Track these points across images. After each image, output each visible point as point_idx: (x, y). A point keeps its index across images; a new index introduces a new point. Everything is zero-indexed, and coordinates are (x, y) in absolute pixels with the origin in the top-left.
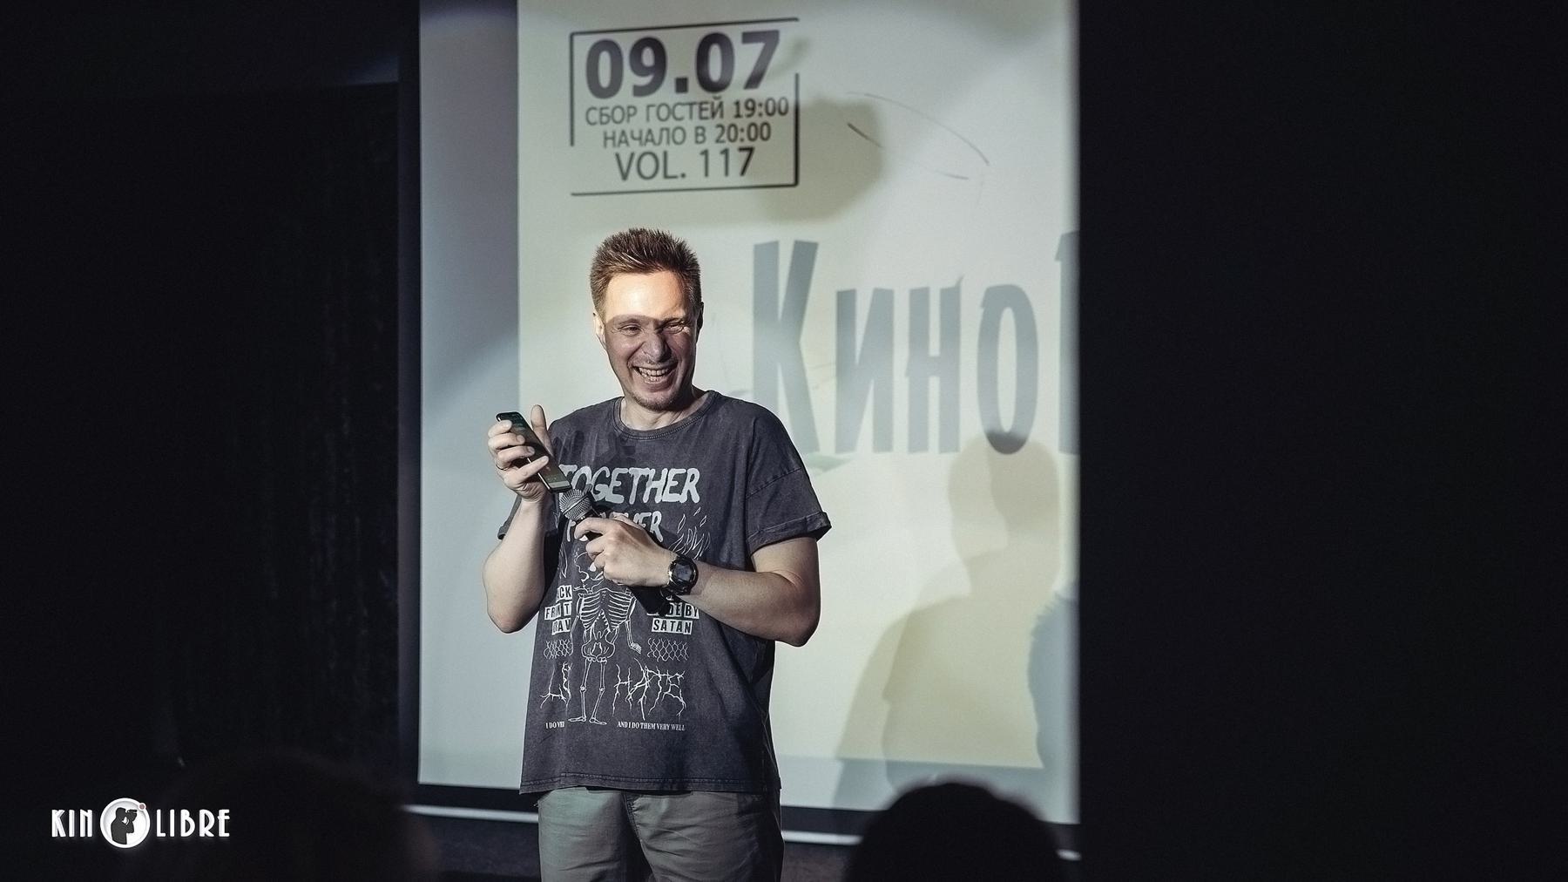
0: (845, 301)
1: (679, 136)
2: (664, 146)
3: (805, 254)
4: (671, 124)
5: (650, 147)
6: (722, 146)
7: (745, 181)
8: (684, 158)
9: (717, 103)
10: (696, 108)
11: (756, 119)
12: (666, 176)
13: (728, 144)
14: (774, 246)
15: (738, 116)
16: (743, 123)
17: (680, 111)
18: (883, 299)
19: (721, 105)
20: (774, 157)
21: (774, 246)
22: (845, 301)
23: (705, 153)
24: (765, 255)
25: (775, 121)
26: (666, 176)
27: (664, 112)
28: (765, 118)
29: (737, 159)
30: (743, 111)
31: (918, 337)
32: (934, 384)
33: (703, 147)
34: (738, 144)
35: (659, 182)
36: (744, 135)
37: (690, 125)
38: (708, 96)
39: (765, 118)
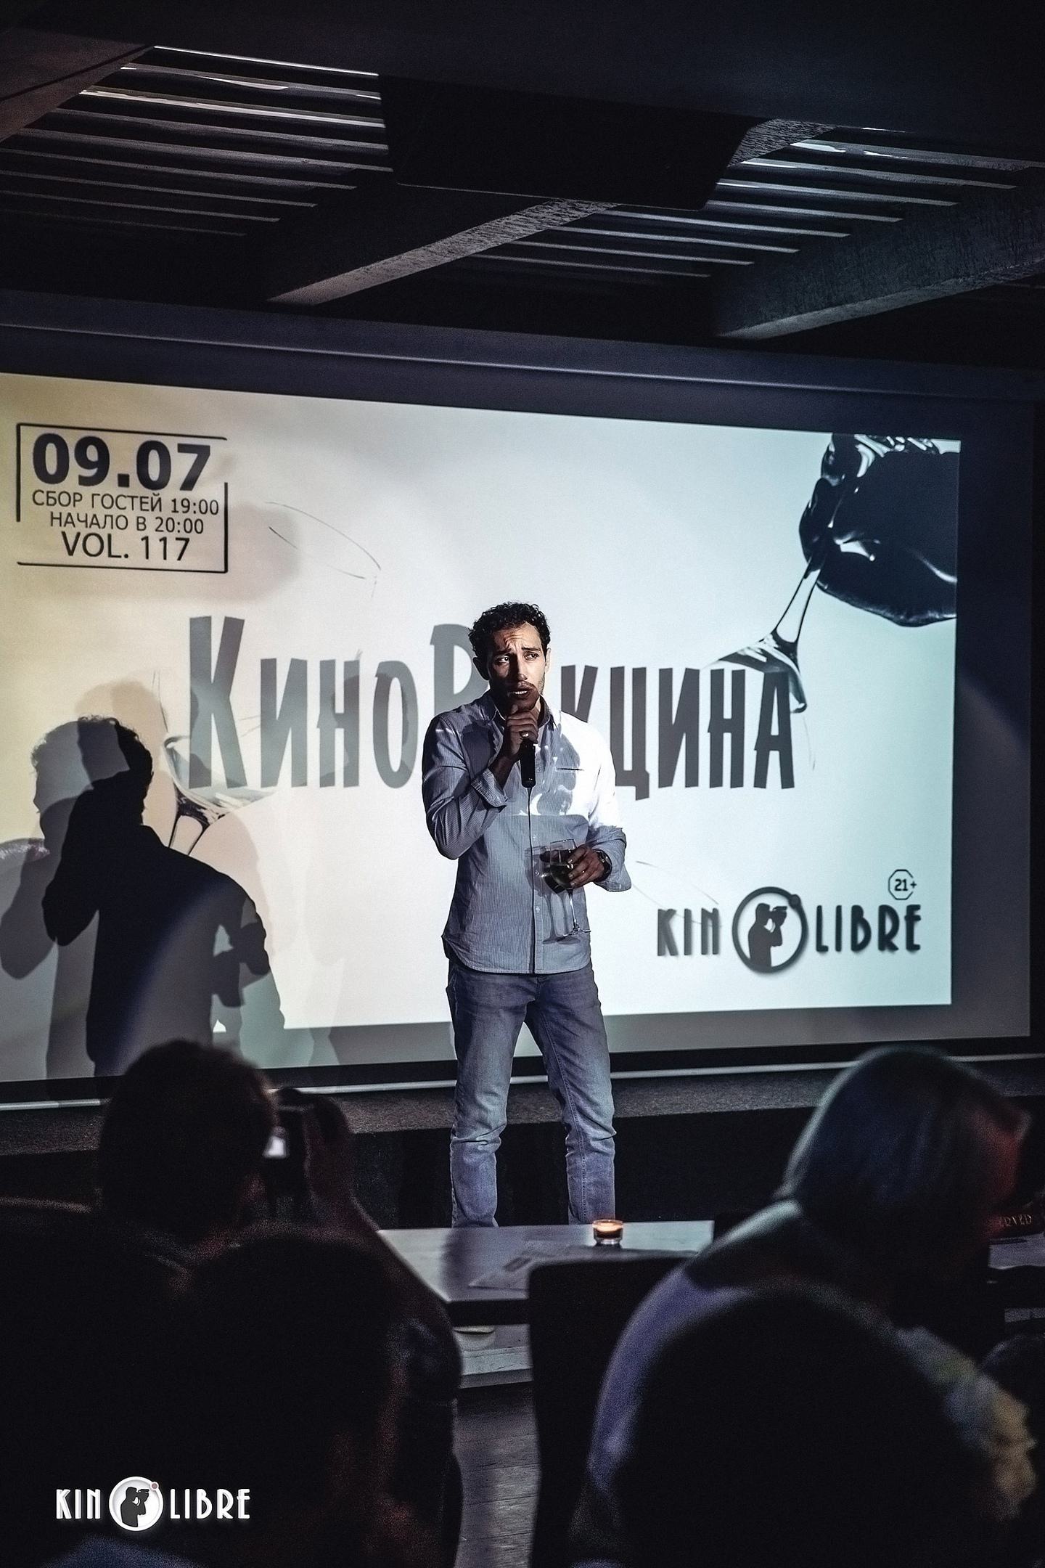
0: (268, 668)
1: (122, 522)
2: (108, 530)
3: (234, 629)
4: (115, 512)
5: (94, 529)
6: (162, 535)
7: (178, 565)
8: (127, 541)
9: (155, 499)
10: (137, 501)
11: (190, 515)
12: (110, 555)
13: (166, 534)
14: (207, 620)
15: (175, 511)
16: (180, 517)
17: (122, 502)
18: (298, 668)
19: (160, 500)
20: (205, 548)
21: (207, 620)
22: (268, 668)
23: (146, 539)
24: (200, 627)
25: (207, 518)
26: (110, 555)
27: (108, 502)
28: (199, 516)
29: (174, 547)
30: (179, 507)
31: (327, 697)
32: (339, 734)
33: (143, 534)
34: (175, 534)
35: (104, 559)
36: (181, 527)
37: (132, 515)
38: (149, 493)
39: (199, 516)
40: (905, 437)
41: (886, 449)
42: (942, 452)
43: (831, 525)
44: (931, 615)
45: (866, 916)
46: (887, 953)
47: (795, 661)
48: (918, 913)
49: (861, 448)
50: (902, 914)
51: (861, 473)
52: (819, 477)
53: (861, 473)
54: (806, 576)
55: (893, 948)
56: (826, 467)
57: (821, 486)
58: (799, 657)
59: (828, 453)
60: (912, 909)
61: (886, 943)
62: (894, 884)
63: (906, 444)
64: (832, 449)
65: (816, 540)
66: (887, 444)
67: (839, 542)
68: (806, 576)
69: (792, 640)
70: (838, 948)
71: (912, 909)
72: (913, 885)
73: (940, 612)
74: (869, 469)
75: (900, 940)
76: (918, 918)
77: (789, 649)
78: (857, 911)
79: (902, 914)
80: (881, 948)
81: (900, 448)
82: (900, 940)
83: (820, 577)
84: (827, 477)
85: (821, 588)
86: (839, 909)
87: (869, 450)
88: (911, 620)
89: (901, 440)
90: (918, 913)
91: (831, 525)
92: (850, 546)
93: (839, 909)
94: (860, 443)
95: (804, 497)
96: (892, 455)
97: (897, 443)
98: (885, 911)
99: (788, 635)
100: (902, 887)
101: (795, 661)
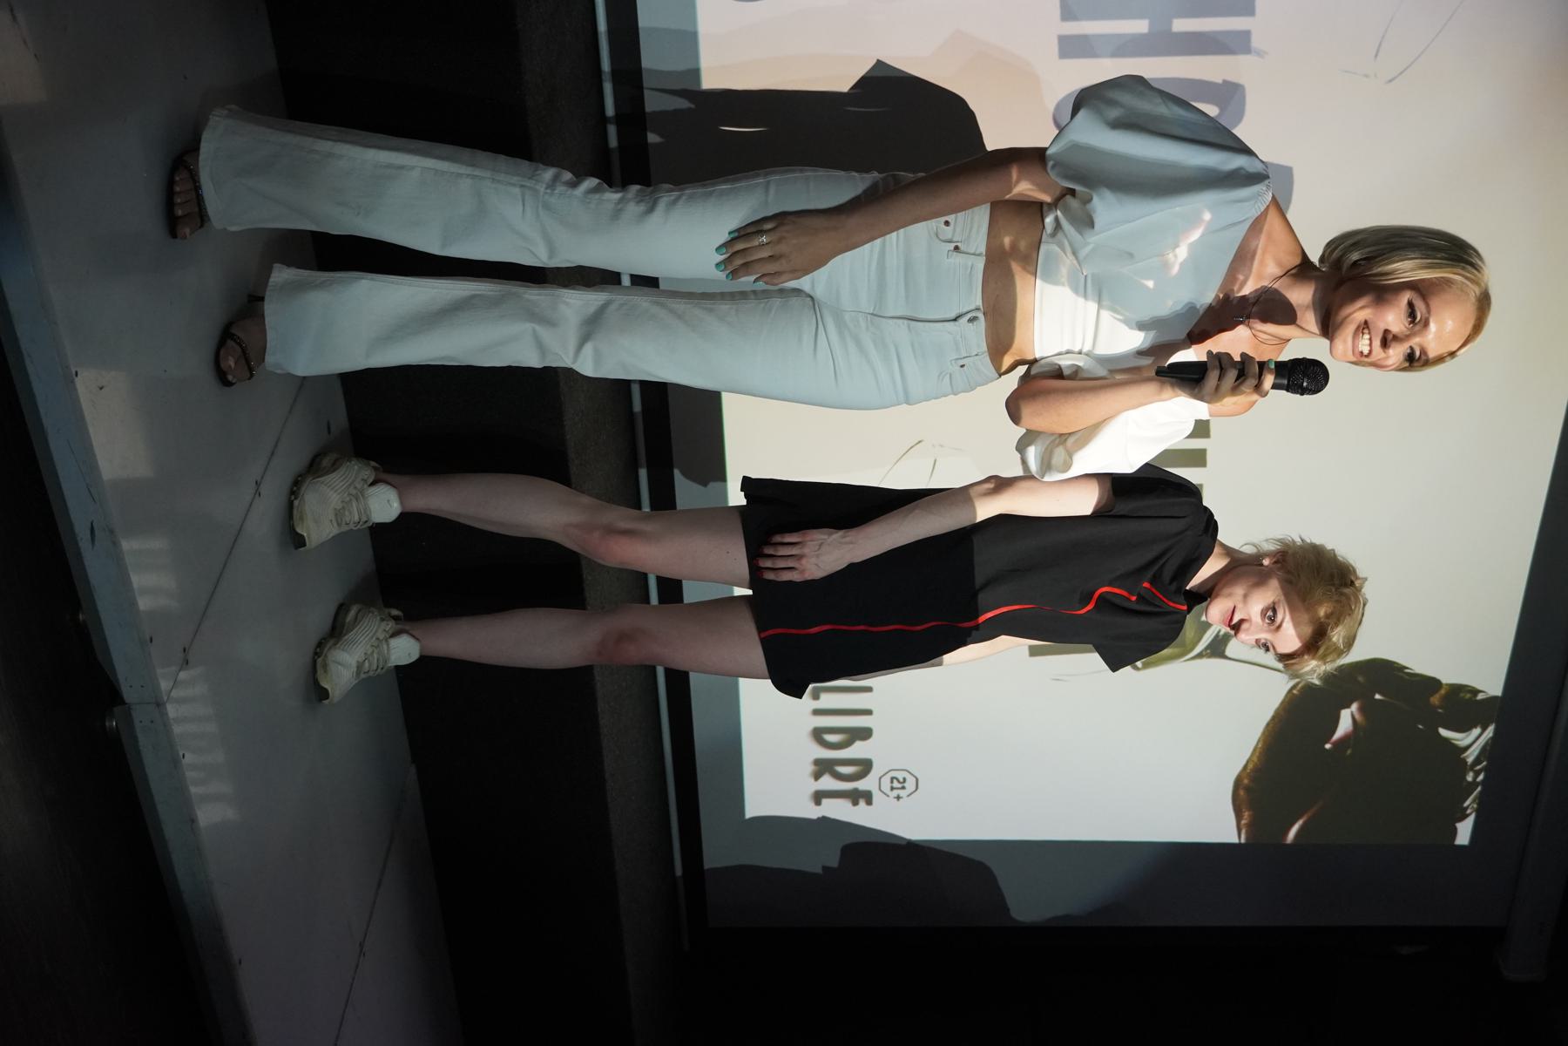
41: (1470, 760)
42: (1459, 825)
43: (1378, 697)
44: (1246, 814)
45: (858, 744)
46: (811, 768)
47: (1200, 656)
48: (862, 803)
50: (861, 785)
51: (1443, 732)
52: (1444, 681)
53: (1443, 732)
55: (817, 776)
56: (1457, 689)
57: (1432, 684)
58: (1205, 661)
60: (868, 797)
61: (823, 768)
62: (900, 776)
65: (1360, 679)
67: (1354, 707)
69: (1228, 652)
70: (817, 712)
71: (868, 797)
72: (898, 798)
73: (1249, 826)
74: (1447, 741)
75: (827, 783)
76: (855, 803)
77: (1217, 649)
78: (865, 734)
79: (861, 785)
80: (817, 762)
81: (1470, 778)
82: (827, 783)
84: (1443, 692)
86: (868, 712)
87: (1473, 741)
88: (1242, 793)
90: (862, 803)
91: (1378, 697)
92: (1346, 722)
93: (868, 712)
95: (1419, 662)
98: (865, 766)
99: (1233, 648)
100: (896, 784)
101: (1200, 656)
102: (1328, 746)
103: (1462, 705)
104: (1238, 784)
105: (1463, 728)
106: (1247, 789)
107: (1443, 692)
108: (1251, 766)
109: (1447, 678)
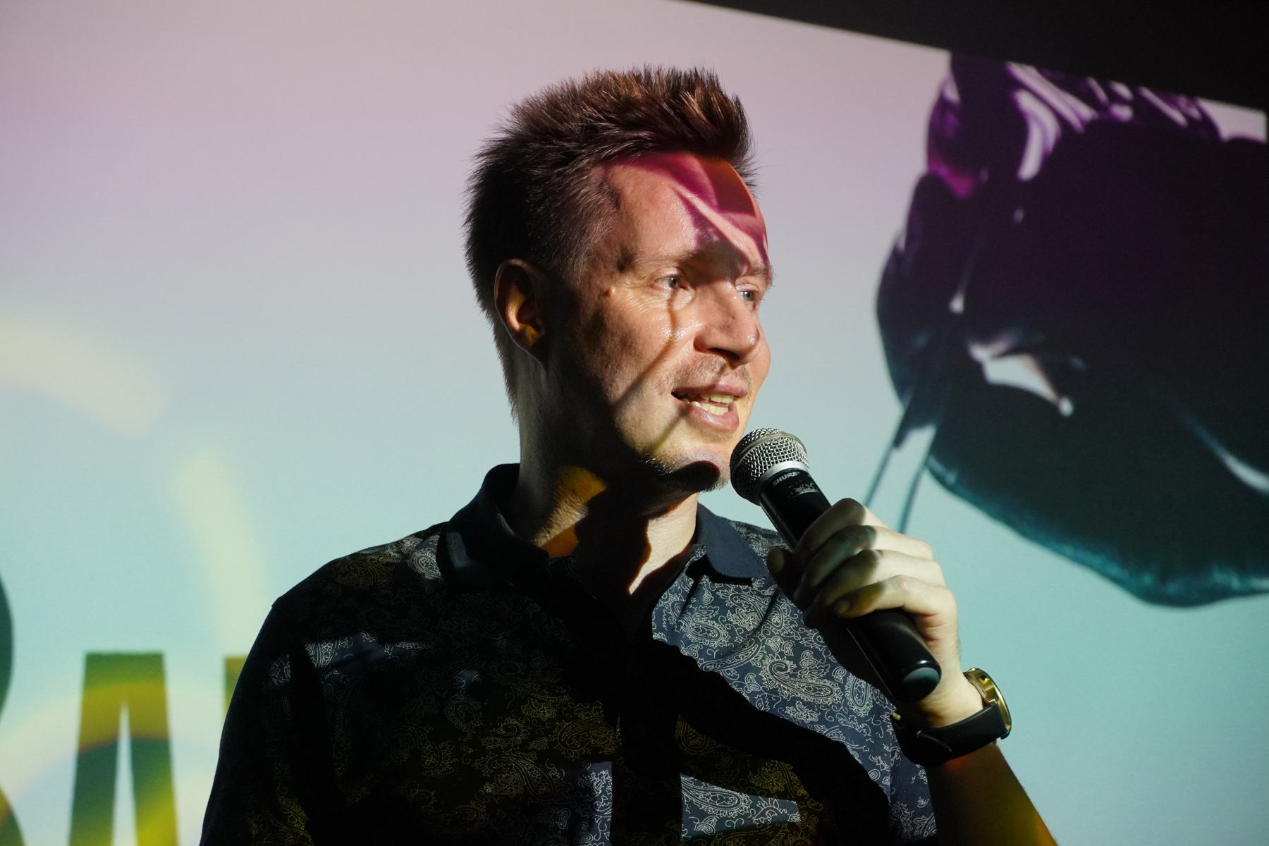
40: (1133, 86)
41: (1086, 112)
43: (957, 305)
49: (1025, 101)
51: (1030, 166)
53: (1030, 166)
54: (899, 440)
59: (942, 105)
63: (1137, 103)
64: (953, 95)
65: (921, 341)
66: (1088, 97)
67: (981, 353)
68: (899, 440)
74: (1050, 161)
81: (1124, 113)
83: (937, 449)
84: (943, 171)
85: (940, 479)
87: (1046, 110)
88: (1172, 588)
89: (1123, 90)
91: (957, 305)
92: (1012, 371)
94: (1021, 86)
96: (1103, 126)
97: (1115, 98)
102: (1066, 407)
103: (970, 132)
104: (1153, 597)
105: (1018, 127)
106: (1164, 577)
107: (943, 171)
108: (1115, 570)
109: (910, 161)
